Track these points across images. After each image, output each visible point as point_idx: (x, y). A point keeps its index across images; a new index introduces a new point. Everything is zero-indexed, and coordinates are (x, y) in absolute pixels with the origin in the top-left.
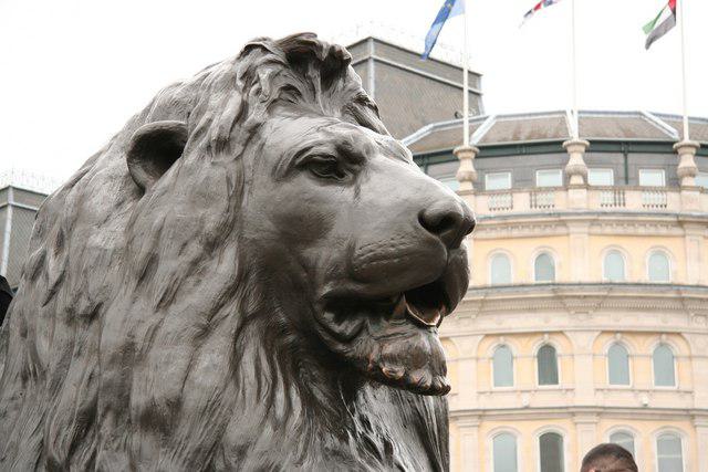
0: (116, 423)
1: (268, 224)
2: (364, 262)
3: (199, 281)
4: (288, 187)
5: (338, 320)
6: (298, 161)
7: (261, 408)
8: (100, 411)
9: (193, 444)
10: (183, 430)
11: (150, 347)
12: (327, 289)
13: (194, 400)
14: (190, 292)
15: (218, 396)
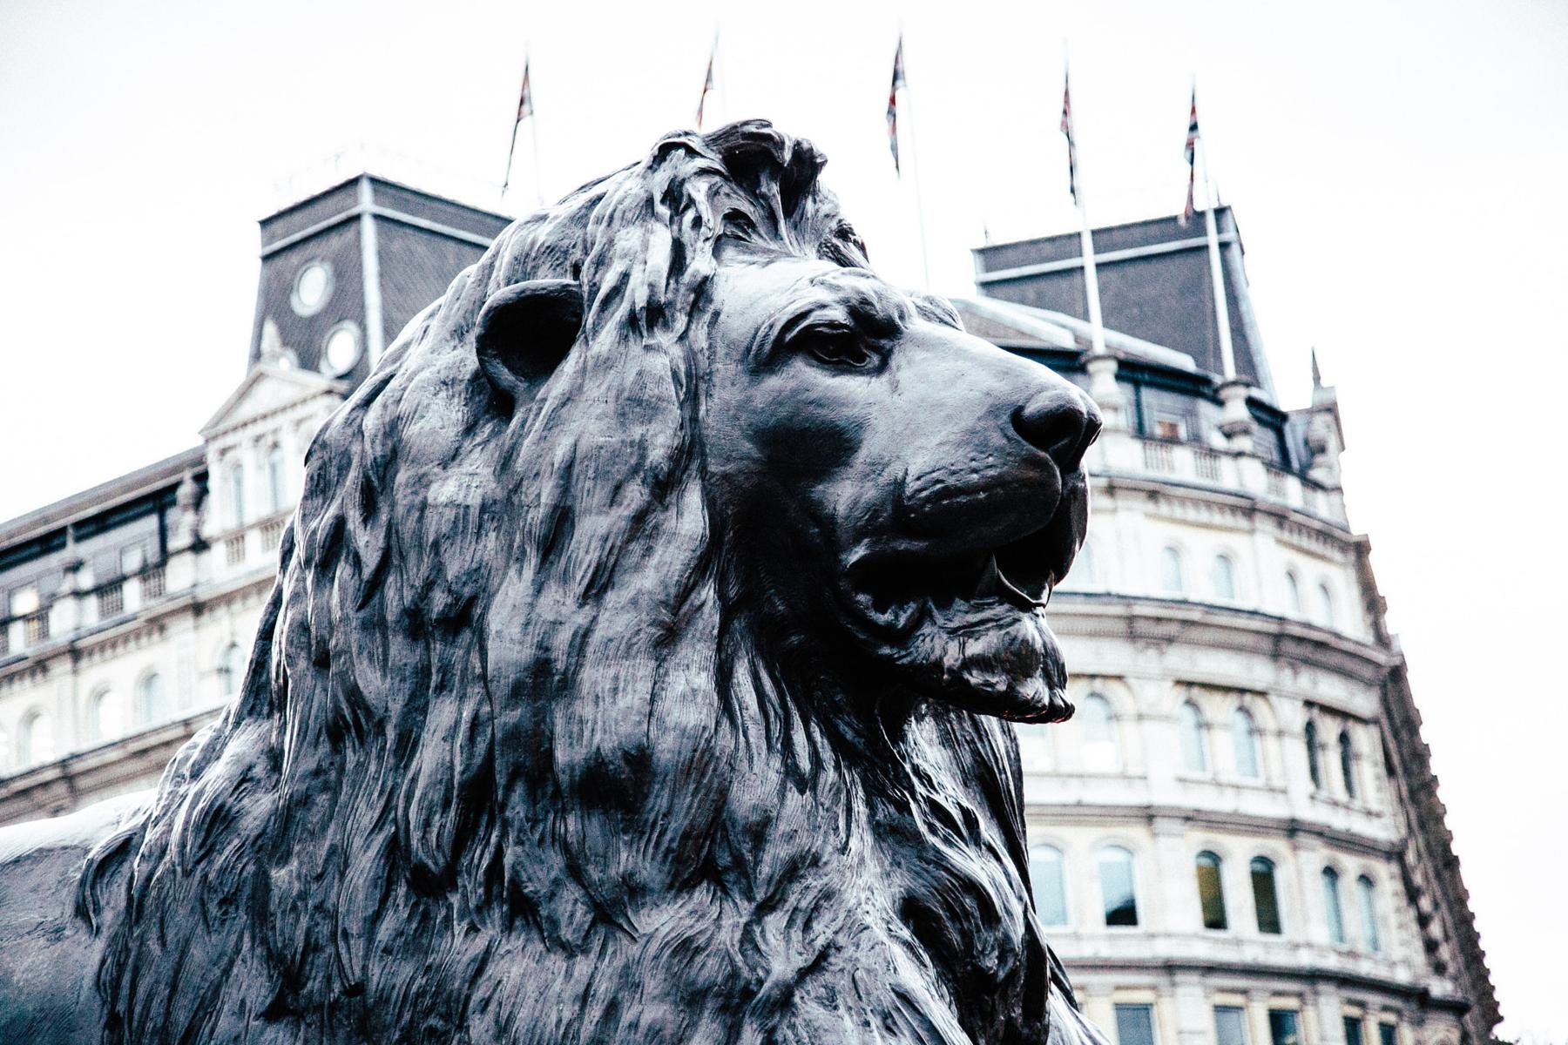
0: (532, 797)
1: (747, 447)
2: (927, 499)
3: (648, 551)
4: (774, 383)
6: (789, 337)
7: (776, 763)
8: (501, 779)
9: (677, 824)
10: (659, 801)
11: (579, 666)
12: (858, 553)
14: (637, 568)
15: (708, 741)
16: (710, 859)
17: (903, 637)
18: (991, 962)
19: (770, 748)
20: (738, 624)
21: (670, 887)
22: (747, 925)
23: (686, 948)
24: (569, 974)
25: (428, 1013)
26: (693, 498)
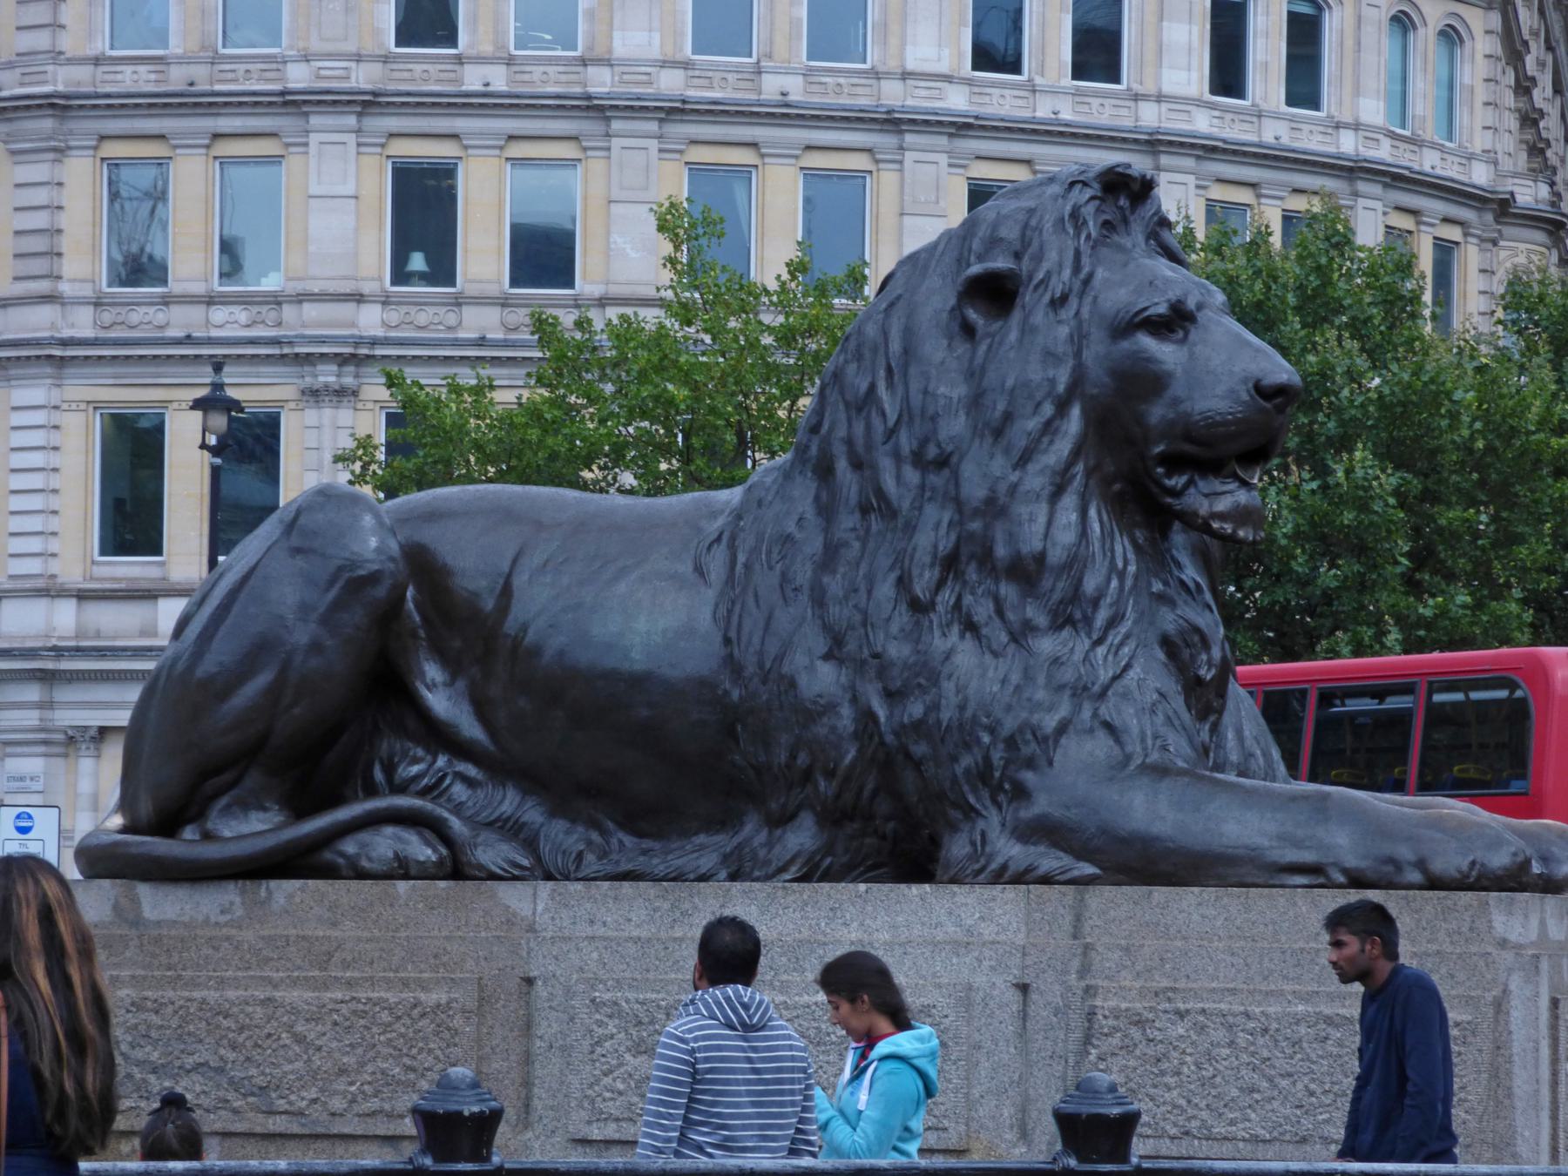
1: (1106, 380)
3: (1051, 442)
4: (1125, 345)
5: (1169, 475)
6: (1137, 320)
8: (964, 558)
9: (1057, 596)
10: (1047, 583)
12: (1159, 449)
13: (1056, 556)
14: (1046, 451)
16: (1071, 615)
17: (1177, 493)
18: (1202, 672)
19: (1105, 554)
20: (1092, 482)
21: (1050, 628)
22: (1087, 652)
23: (1056, 661)
24: (996, 669)
25: (917, 675)
26: (1076, 412)
